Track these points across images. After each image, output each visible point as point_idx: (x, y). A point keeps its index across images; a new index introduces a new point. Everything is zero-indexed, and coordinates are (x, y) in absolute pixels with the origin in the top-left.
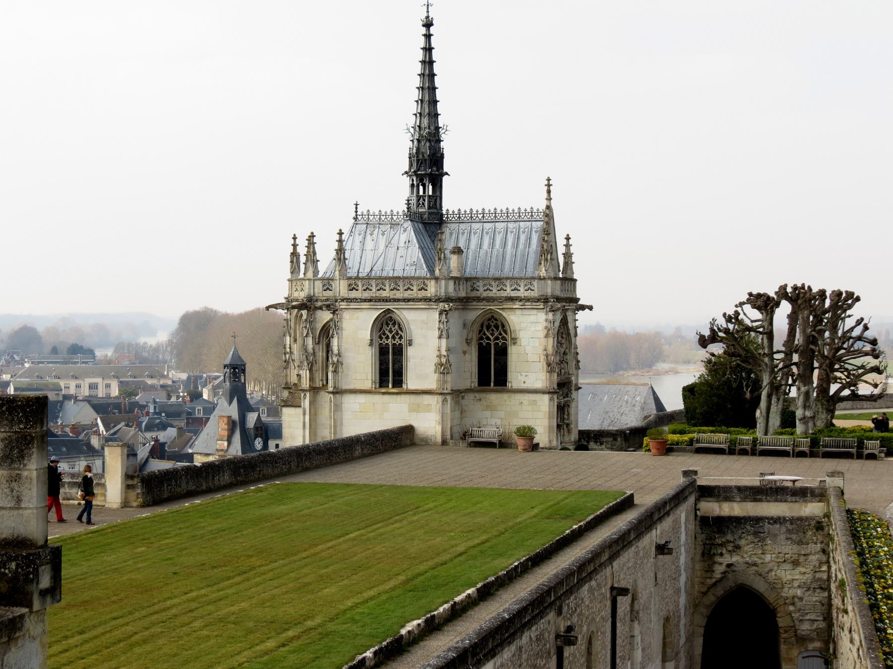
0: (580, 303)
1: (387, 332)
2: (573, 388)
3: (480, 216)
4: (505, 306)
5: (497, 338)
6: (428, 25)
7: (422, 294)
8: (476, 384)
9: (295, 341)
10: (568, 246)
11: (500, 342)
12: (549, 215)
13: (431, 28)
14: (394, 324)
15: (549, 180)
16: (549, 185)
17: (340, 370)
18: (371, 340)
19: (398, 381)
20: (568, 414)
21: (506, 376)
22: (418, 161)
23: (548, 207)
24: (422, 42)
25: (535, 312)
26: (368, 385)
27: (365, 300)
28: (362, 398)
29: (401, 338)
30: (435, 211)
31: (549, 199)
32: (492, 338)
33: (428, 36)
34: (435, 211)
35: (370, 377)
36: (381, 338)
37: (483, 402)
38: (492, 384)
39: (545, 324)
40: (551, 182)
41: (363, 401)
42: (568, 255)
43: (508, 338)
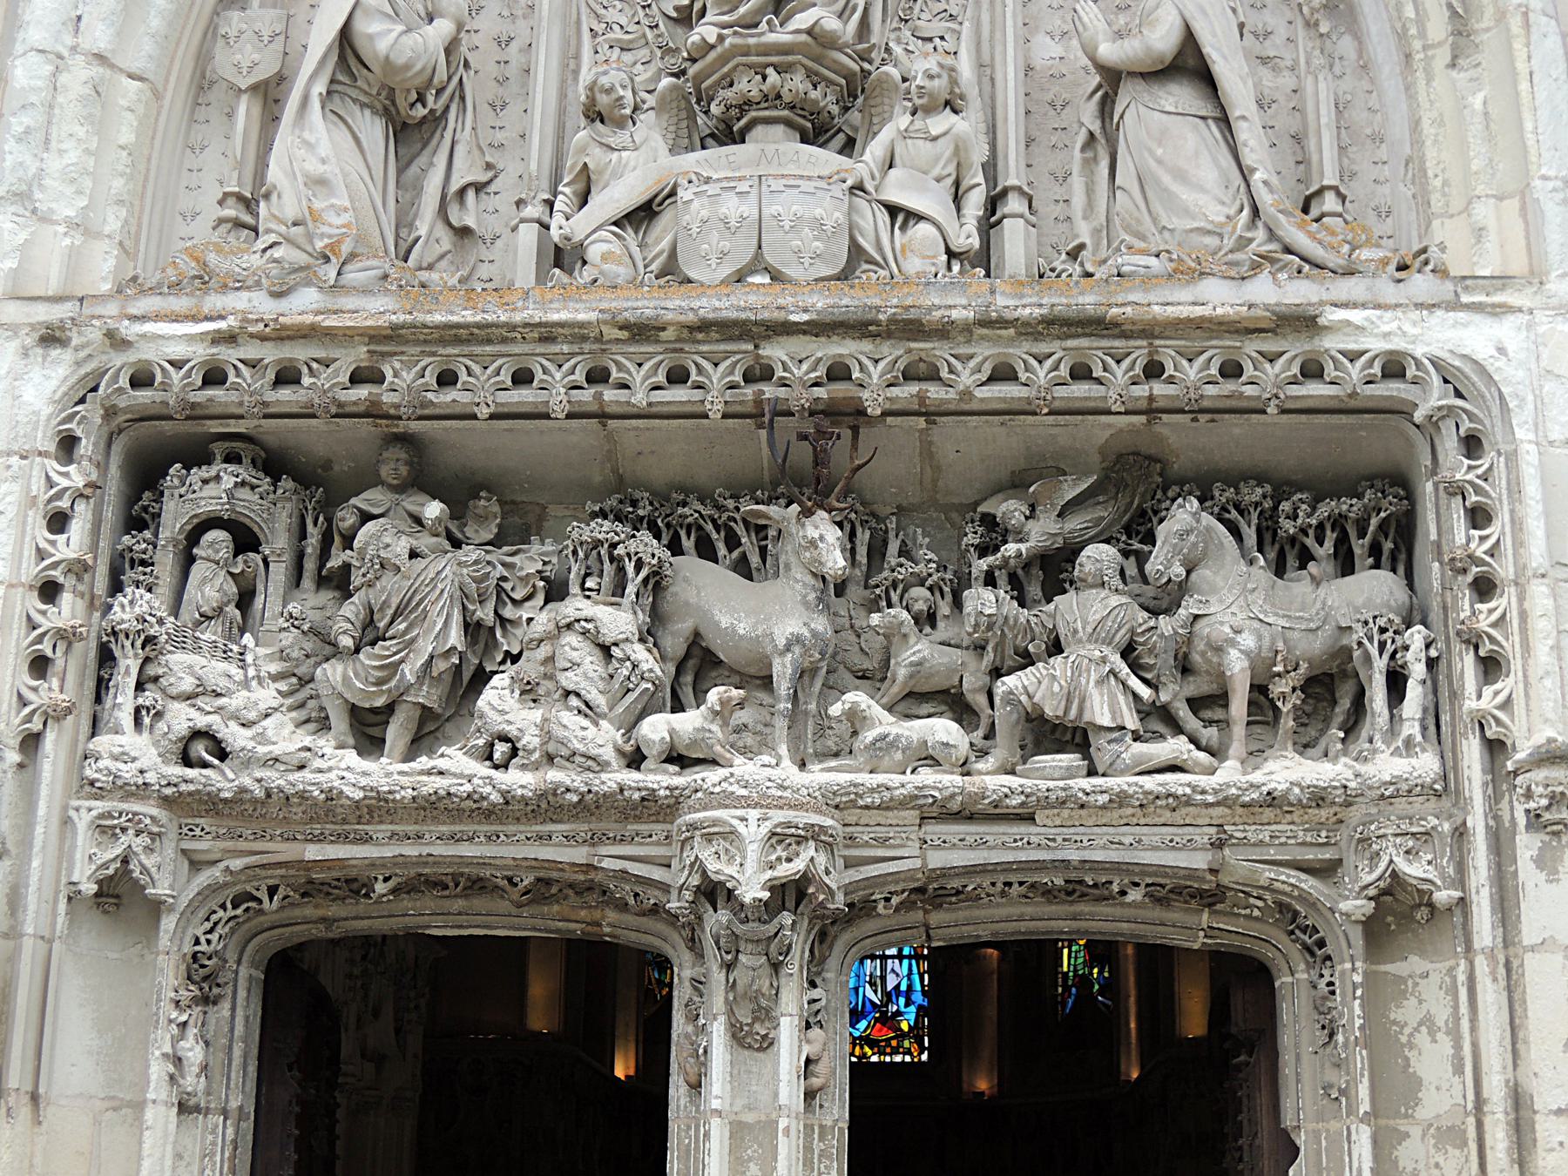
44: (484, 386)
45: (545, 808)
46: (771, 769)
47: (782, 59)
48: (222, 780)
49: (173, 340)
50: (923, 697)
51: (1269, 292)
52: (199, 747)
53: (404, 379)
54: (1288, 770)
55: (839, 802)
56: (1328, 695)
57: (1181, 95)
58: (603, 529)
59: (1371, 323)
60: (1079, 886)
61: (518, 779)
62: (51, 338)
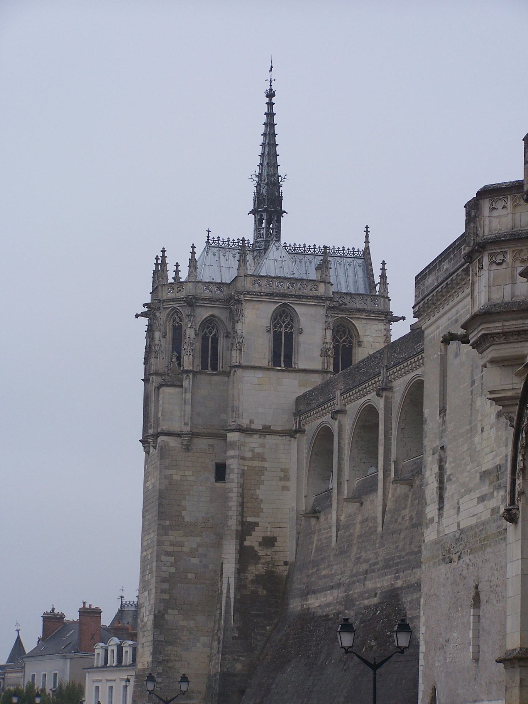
1: (281, 322)
3: (312, 250)
5: (344, 341)
6: (271, 95)
7: (313, 293)
9: (164, 337)
11: (347, 345)
12: (366, 252)
13: (274, 100)
14: (286, 316)
15: (367, 227)
16: (367, 232)
19: (289, 362)
22: (268, 199)
23: (367, 248)
25: (376, 322)
27: (267, 294)
28: (260, 374)
29: (292, 327)
31: (367, 242)
33: (270, 104)
35: (267, 357)
36: (275, 326)
40: (369, 229)
41: (261, 376)
43: (355, 341)
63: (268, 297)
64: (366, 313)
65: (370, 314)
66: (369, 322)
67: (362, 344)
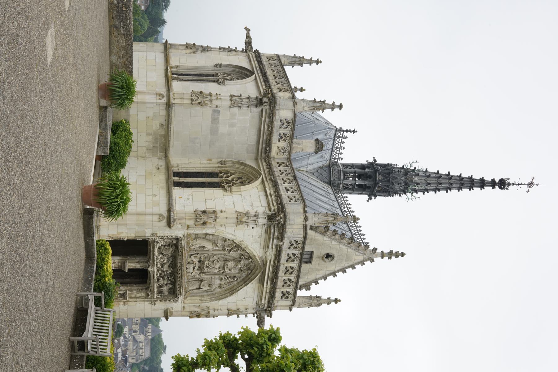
0: (267, 319)
2: (169, 305)
3: (346, 209)
4: (266, 183)
6: (503, 184)
8: (175, 169)
10: (329, 301)
16: (397, 255)
17: (189, 51)
18: (220, 66)
20: (136, 297)
21: (185, 187)
24: (488, 178)
25: (265, 204)
26: (174, 62)
30: (342, 178)
31: (383, 255)
32: (230, 179)
33: (493, 184)
34: (342, 178)
37: (155, 171)
38: (176, 178)
39: (252, 212)
41: (157, 60)
42: (317, 301)
44: (179, 257)
45: (154, 259)
46: (156, 270)
47: (203, 268)
48: (155, 244)
49: (183, 242)
50: (161, 274)
51: (183, 293)
52: (158, 242)
53: (180, 253)
54: (156, 290)
55: (154, 272)
56: (160, 292)
57: (198, 287)
58: (171, 260)
59: (181, 298)
60: (150, 280)
61: (155, 258)
62: (184, 236)
63: (256, 63)
64: (275, 192)
65: (275, 196)
66: (263, 199)
67: (229, 193)
